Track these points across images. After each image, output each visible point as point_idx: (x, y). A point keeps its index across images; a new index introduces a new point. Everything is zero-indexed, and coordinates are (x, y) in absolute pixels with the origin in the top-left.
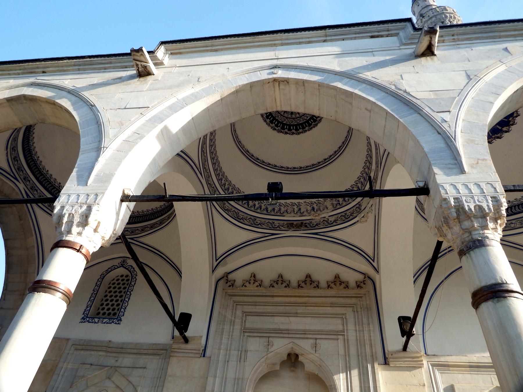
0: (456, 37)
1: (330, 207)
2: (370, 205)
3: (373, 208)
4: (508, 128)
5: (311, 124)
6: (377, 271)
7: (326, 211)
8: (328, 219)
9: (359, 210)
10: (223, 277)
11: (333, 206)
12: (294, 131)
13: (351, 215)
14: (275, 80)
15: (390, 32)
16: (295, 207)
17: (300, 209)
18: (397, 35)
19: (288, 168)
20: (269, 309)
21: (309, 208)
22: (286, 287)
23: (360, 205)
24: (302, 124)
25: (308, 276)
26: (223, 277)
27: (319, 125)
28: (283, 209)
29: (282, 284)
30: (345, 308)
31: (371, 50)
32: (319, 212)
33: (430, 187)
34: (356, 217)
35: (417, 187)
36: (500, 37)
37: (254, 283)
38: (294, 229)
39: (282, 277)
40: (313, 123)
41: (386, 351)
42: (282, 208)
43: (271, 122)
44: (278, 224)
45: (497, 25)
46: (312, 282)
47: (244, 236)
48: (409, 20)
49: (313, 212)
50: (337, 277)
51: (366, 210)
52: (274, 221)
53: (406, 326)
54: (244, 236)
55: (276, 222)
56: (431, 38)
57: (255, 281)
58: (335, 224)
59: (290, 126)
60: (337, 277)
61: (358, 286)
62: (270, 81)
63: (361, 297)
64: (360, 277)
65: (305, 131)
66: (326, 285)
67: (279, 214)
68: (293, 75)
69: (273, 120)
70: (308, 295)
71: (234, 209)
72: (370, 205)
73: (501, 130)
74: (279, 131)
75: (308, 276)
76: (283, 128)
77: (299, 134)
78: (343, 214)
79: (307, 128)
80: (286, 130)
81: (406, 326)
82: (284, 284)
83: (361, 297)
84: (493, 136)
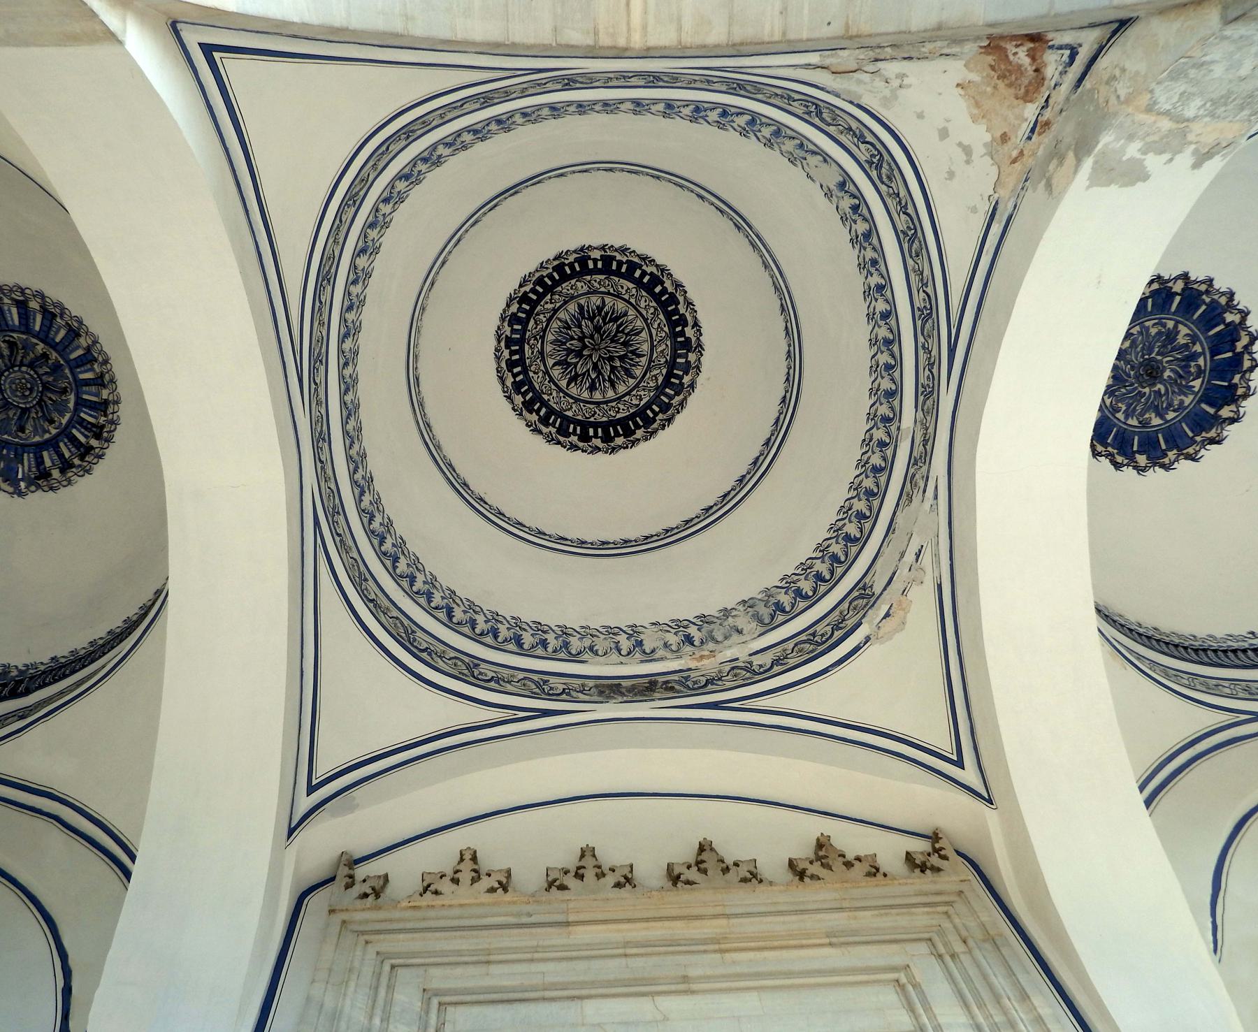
1: (749, 626)
3: (927, 558)
4: (1233, 407)
7: (735, 638)
8: (751, 663)
9: (861, 602)
10: (333, 879)
11: (761, 621)
12: (597, 442)
13: (837, 627)
16: (622, 638)
17: (640, 644)
20: (554, 972)
22: (618, 885)
24: (623, 422)
26: (333, 879)
27: (678, 418)
29: (600, 875)
30: (895, 947)
32: (711, 646)
34: (859, 625)
37: (474, 881)
40: (660, 416)
43: (528, 406)
44: (561, 687)
47: (435, 711)
49: (688, 649)
50: (822, 844)
51: (897, 585)
52: (546, 677)
54: (435, 711)
55: (552, 680)
57: (477, 877)
58: (776, 669)
59: (585, 425)
66: (790, 876)
67: (562, 655)
70: (719, 910)
71: (395, 613)
72: (910, 557)
73: (1216, 417)
74: (550, 439)
76: (562, 431)
77: (613, 450)
78: (803, 637)
79: (639, 433)
80: (574, 439)
82: (610, 879)
84: (1198, 439)
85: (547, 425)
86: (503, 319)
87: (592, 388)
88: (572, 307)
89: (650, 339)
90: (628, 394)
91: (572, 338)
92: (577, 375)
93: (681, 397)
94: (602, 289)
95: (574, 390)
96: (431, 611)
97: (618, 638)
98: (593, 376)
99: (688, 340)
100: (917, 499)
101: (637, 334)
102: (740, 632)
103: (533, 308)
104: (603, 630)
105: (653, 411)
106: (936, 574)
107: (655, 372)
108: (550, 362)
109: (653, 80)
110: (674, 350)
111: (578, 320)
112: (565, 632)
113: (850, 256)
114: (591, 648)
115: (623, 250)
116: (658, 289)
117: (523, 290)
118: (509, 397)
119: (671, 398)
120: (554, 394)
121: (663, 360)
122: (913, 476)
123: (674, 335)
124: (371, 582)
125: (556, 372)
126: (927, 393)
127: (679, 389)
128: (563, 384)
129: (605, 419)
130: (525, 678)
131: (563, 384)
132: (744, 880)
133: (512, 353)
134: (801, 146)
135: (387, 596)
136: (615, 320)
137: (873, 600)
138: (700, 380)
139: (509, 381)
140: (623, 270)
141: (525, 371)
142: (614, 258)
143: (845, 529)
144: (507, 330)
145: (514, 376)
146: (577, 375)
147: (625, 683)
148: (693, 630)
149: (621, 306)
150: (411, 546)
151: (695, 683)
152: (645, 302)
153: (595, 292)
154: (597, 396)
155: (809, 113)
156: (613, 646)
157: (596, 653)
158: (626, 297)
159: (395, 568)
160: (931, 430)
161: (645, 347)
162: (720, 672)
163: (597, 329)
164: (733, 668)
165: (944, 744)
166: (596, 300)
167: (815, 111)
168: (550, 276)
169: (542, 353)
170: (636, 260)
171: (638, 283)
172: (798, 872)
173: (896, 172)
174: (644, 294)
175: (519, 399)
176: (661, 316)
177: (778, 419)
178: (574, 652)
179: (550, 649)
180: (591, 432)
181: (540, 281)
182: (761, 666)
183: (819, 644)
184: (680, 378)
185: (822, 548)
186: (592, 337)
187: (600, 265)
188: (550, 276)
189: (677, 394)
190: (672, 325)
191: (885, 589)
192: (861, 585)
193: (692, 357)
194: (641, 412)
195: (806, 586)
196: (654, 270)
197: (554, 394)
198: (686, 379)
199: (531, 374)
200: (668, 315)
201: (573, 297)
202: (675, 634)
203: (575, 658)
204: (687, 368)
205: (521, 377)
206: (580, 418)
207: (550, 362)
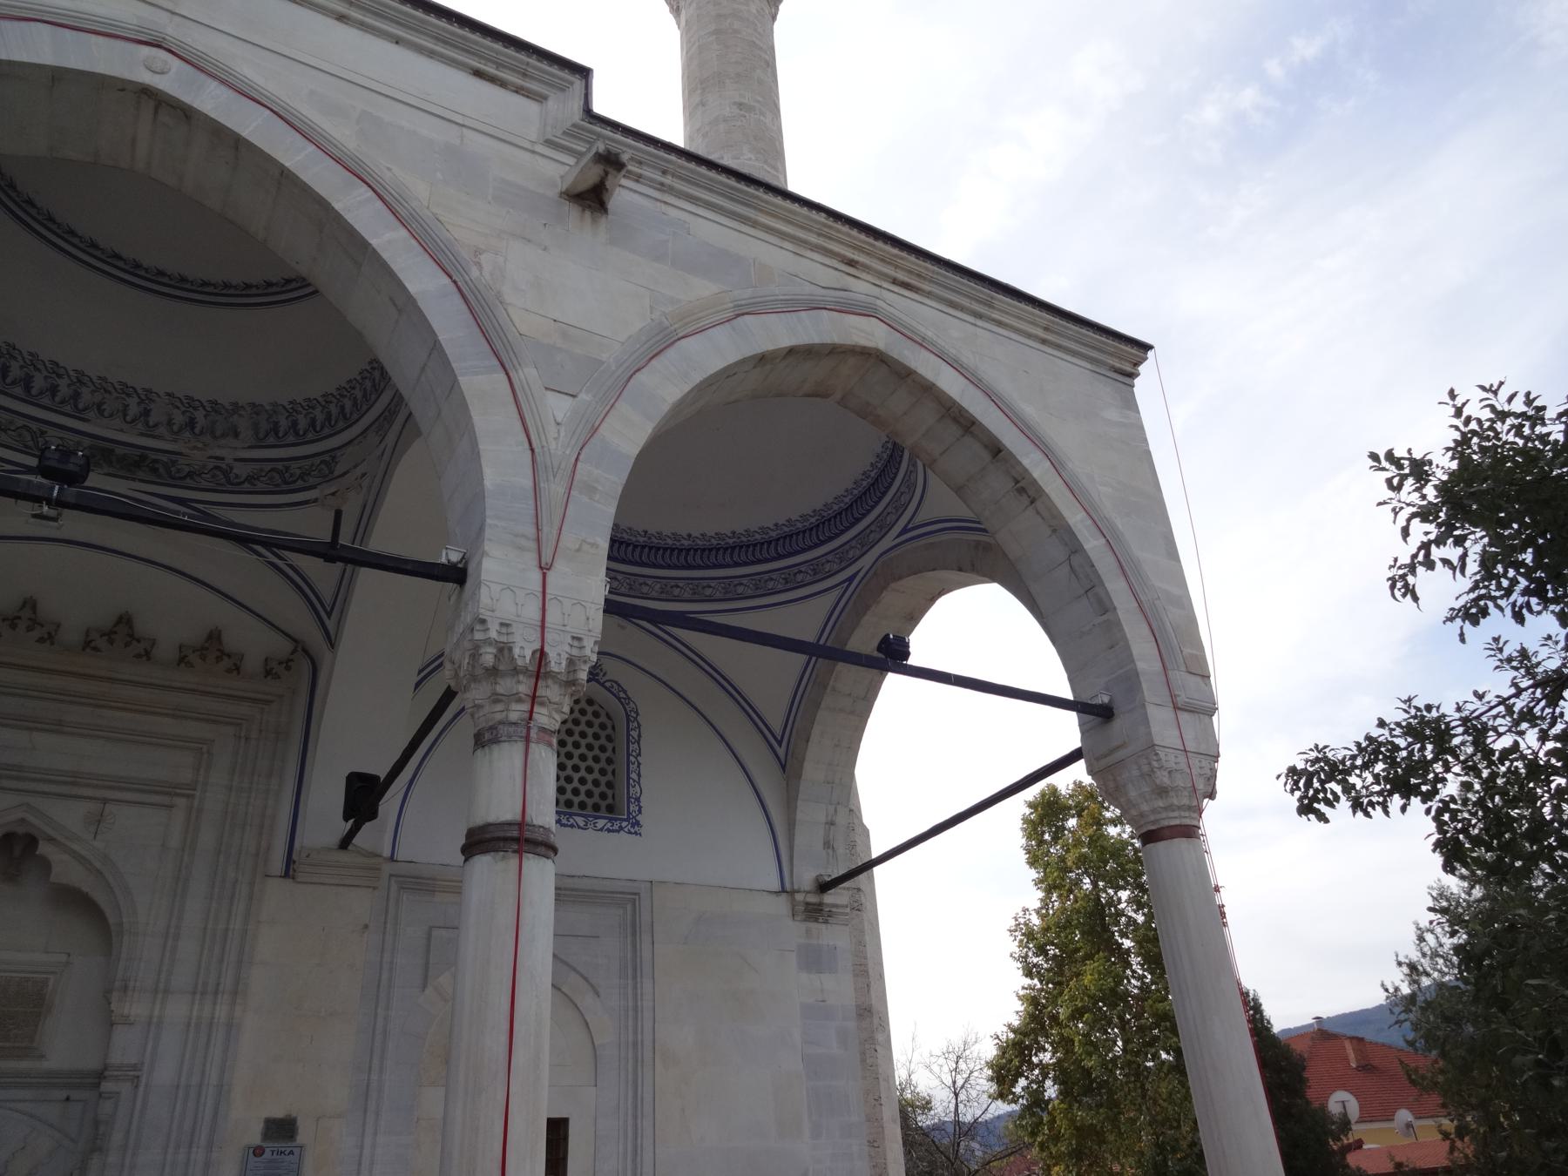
0: (668, 180)
2: (359, 471)
6: (332, 643)
13: (301, 477)
14: (146, 92)
15: (527, 85)
17: (147, 413)
18: (540, 98)
19: (138, 266)
21: (179, 419)
22: (41, 640)
23: (334, 458)
25: (125, 620)
28: (86, 396)
29: (29, 629)
31: (459, 119)
33: (470, 570)
35: (444, 560)
36: (755, 224)
38: (111, 470)
39: (34, 608)
41: (297, 845)
42: (85, 391)
45: (760, 193)
46: (132, 637)
48: (584, 73)
49: (187, 434)
50: (214, 637)
52: (45, 428)
53: (363, 797)
55: (51, 431)
56: (607, 173)
58: (246, 486)
60: (214, 637)
61: (268, 673)
63: (268, 702)
64: (283, 647)
68: (210, 100)
75: (125, 620)
78: (279, 466)
81: (363, 797)
82: (36, 634)
83: (268, 702)
97: (129, 401)
102: (236, 435)
112: (80, 379)
130: (24, 426)
132: (138, 656)
148: (199, 415)
151: (179, 471)
157: (101, 412)
164: (217, 468)
165: (328, 601)
178: (81, 406)
179: (57, 399)
182: (237, 476)
183: (286, 483)
195: (303, 424)
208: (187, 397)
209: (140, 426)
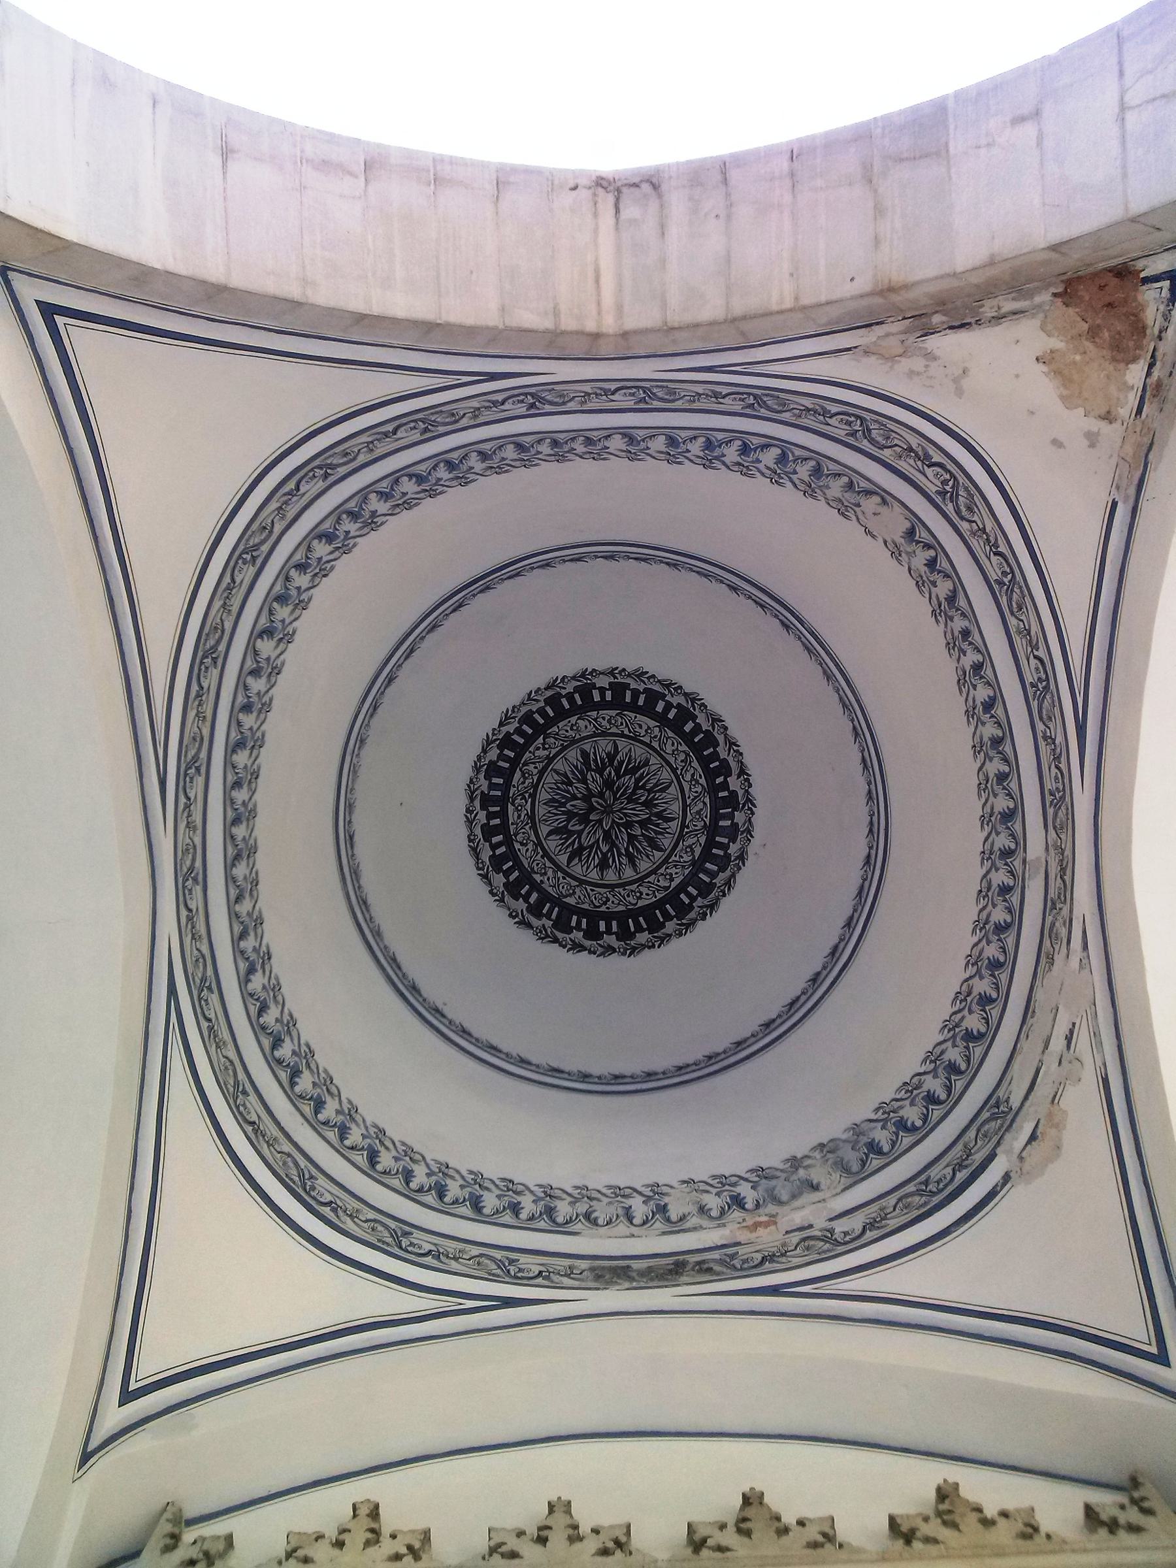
2: (1058, 1044)
3: (1083, 1041)
5: (690, 907)
8: (832, 1231)
11: (846, 1170)
12: (611, 940)
17: (663, 1209)
21: (713, 1202)
24: (647, 911)
27: (725, 903)
28: (563, 1209)
32: (771, 1208)
34: (991, 1157)
40: (700, 901)
43: (513, 889)
49: (737, 1214)
51: (1043, 1090)
55: (524, 1259)
59: (593, 917)
62: (583, 182)
65: (664, 939)
69: (519, 883)
71: (287, 1147)
72: (1058, 1044)
74: (544, 936)
76: (562, 925)
77: (634, 951)
79: (670, 926)
80: (578, 936)
85: (539, 916)
86: (477, 769)
87: (603, 865)
88: (573, 754)
89: (682, 797)
90: (654, 872)
91: (574, 798)
92: (581, 848)
93: (728, 873)
94: (614, 730)
95: (577, 869)
96: (343, 1150)
97: (629, 1202)
98: (605, 849)
99: (734, 794)
100: (1059, 959)
101: (663, 790)
102: (815, 1188)
103: (519, 756)
104: (608, 1192)
105: (689, 895)
106: (1099, 1063)
107: (691, 841)
108: (544, 830)
109: (645, 395)
110: (715, 810)
111: (581, 772)
112: (549, 1193)
113: (934, 634)
114: (587, 1216)
115: (639, 674)
116: (688, 727)
117: (504, 729)
118: (485, 877)
119: (713, 875)
120: (550, 873)
121: (700, 824)
122: (1053, 924)
123: (713, 789)
124: (253, 1098)
125: (552, 844)
126: (1057, 801)
127: (724, 862)
128: (563, 859)
129: (621, 908)
130: (481, 1255)
131: (563, 859)
133: (490, 816)
134: (850, 486)
135: (278, 1124)
136: (632, 771)
137: (1010, 1117)
138: (752, 849)
139: (486, 854)
140: (641, 702)
141: (508, 841)
142: (626, 686)
143: (964, 1024)
144: (484, 784)
145: (494, 847)
146: (581, 848)
147: (636, 1265)
148: (744, 1190)
149: (639, 752)
150: (322, 1059)
152: (673, 745)
153: (604, 734)
154: (611, 876)
155: (853, 434)
156: (620, 1211)
157: (595, 1223)
158: (647, 739)
159: (293, 1084)
160: (1068, 852)
161: (676, 808)
162: (784, 1245)
163: (608, 784)
166: (605, 745)
167: (862, 429)
168: (542, 712)
169: (532, 816)
170: (657, 688)
171: (662, 719)
172: (901, 1531)
173: (977, 499)
174: (671, 734)
175: (499, 880)
176: (695, 764)
177: (862, 887)
178: (560, 1220)
180: (602, 926)
181: (528, 718)
182: (846, 1234)
183: (933, 1194)
184: (725, 847)
185: (933, 1057)
186: (601, 795)
187: (609, 696)
188: (542, 712)
189: (722, 869)
190: (710, 775)
191: (1026, 1098)
192: (993, 1101)
193: (739, 817)
194: (672, 897)
195: (912, 1114)
196: (681, 700)
197: (550, 873)
198: (733, 849)
199: (517, 846)
200: (704, 762)
201: (574, 742)
202: (718, 1194)
203: (562, 1228)
204: (733, 832)
205: (503, 849)
206: (585, 906)
207: (544, 830)
208: (714, 1177)
209: (658, 1225)
